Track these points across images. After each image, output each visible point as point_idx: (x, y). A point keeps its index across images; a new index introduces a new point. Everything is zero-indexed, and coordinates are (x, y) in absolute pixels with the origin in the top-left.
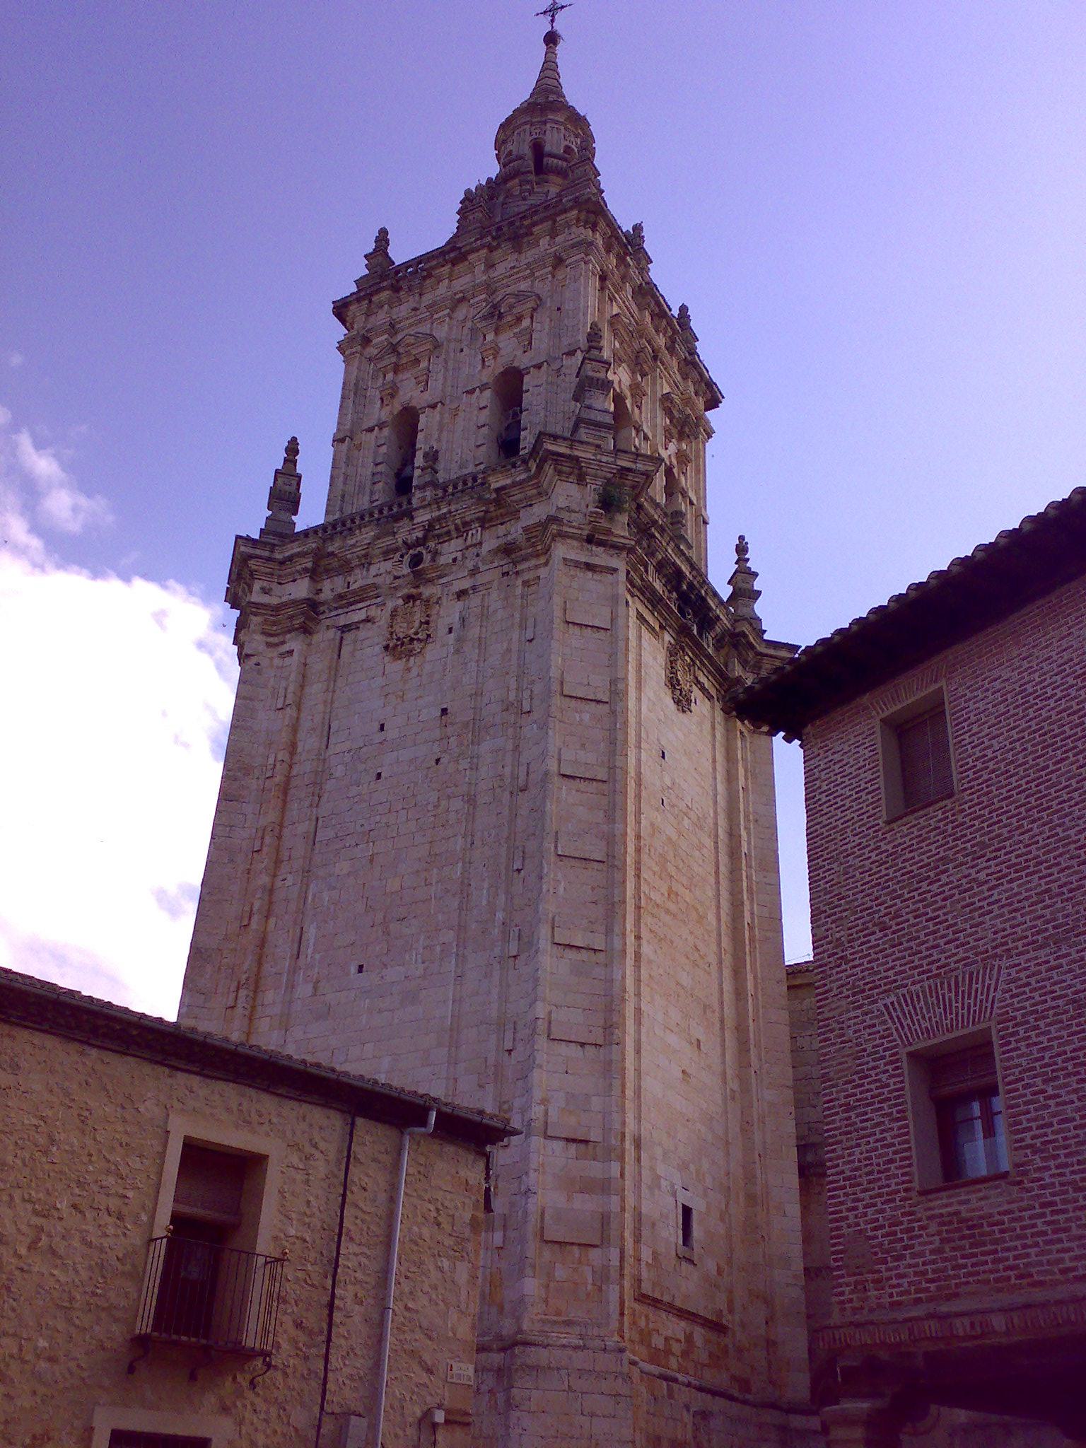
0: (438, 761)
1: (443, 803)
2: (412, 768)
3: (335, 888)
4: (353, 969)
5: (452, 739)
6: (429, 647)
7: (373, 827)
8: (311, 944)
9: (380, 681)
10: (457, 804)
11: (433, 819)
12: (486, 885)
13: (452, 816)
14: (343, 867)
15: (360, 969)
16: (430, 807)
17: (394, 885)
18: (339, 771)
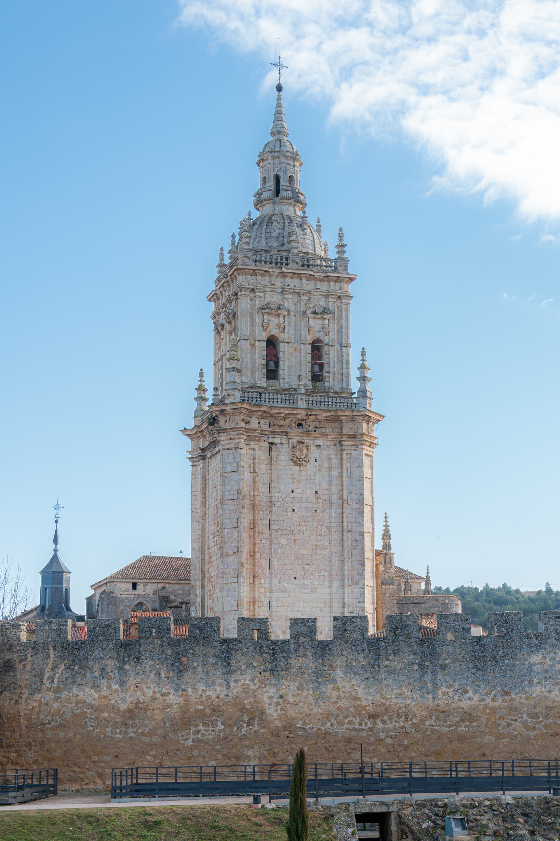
0: (316, 511)
1: (319, 527)
2: (306, 511)
3: (282, 548)
4: (293, 578)
5: (320, 504)
6: (308, 465)
7: (294, 529)
8: (276, 566)
9: (290, 472)
10: (324, 529)
11: (316, 532)
12: (337, 560)
13: (323, 533)
14: (284, 541)
15: (295, 578)
16: (315, 527)
17: (304, 552)
18: (278, 504)
